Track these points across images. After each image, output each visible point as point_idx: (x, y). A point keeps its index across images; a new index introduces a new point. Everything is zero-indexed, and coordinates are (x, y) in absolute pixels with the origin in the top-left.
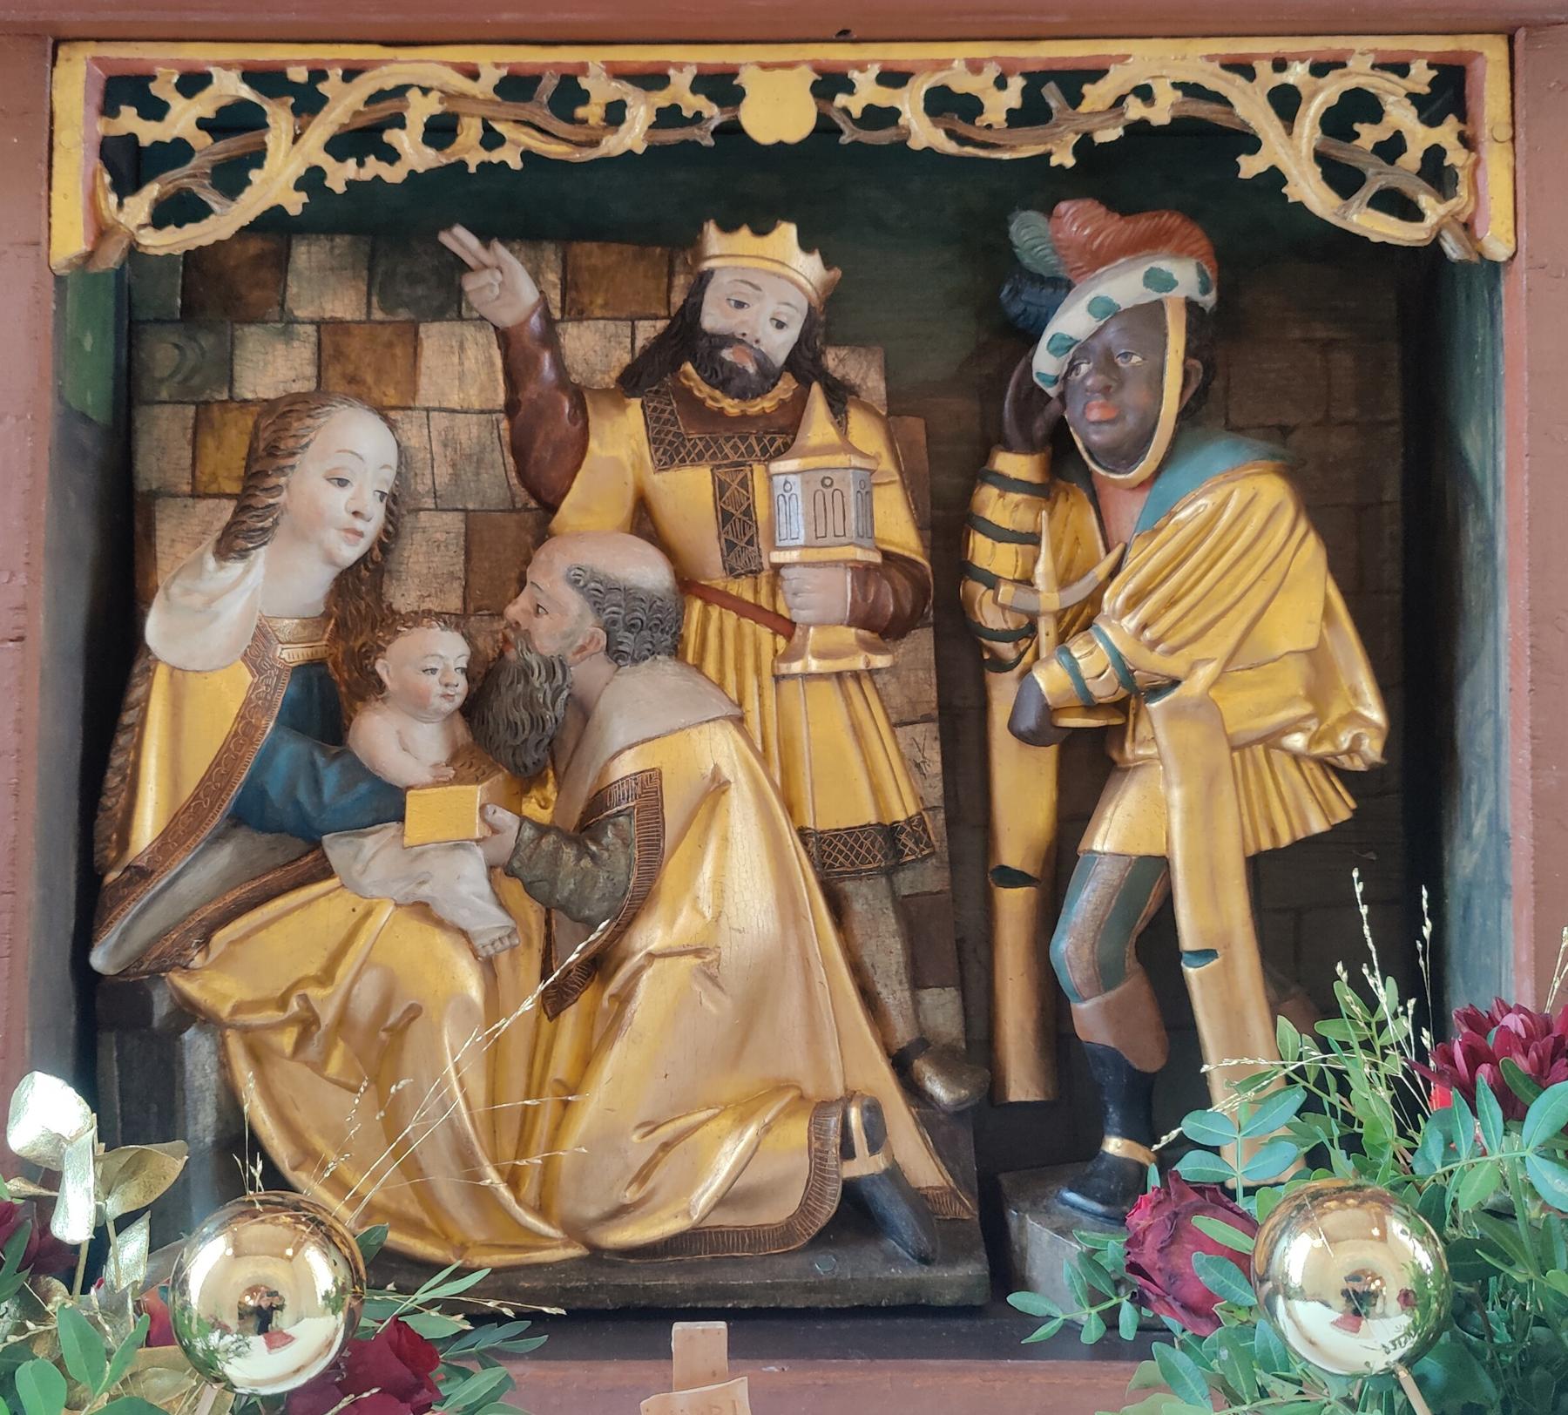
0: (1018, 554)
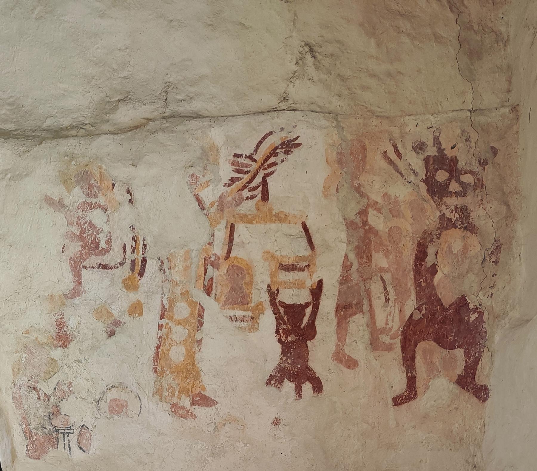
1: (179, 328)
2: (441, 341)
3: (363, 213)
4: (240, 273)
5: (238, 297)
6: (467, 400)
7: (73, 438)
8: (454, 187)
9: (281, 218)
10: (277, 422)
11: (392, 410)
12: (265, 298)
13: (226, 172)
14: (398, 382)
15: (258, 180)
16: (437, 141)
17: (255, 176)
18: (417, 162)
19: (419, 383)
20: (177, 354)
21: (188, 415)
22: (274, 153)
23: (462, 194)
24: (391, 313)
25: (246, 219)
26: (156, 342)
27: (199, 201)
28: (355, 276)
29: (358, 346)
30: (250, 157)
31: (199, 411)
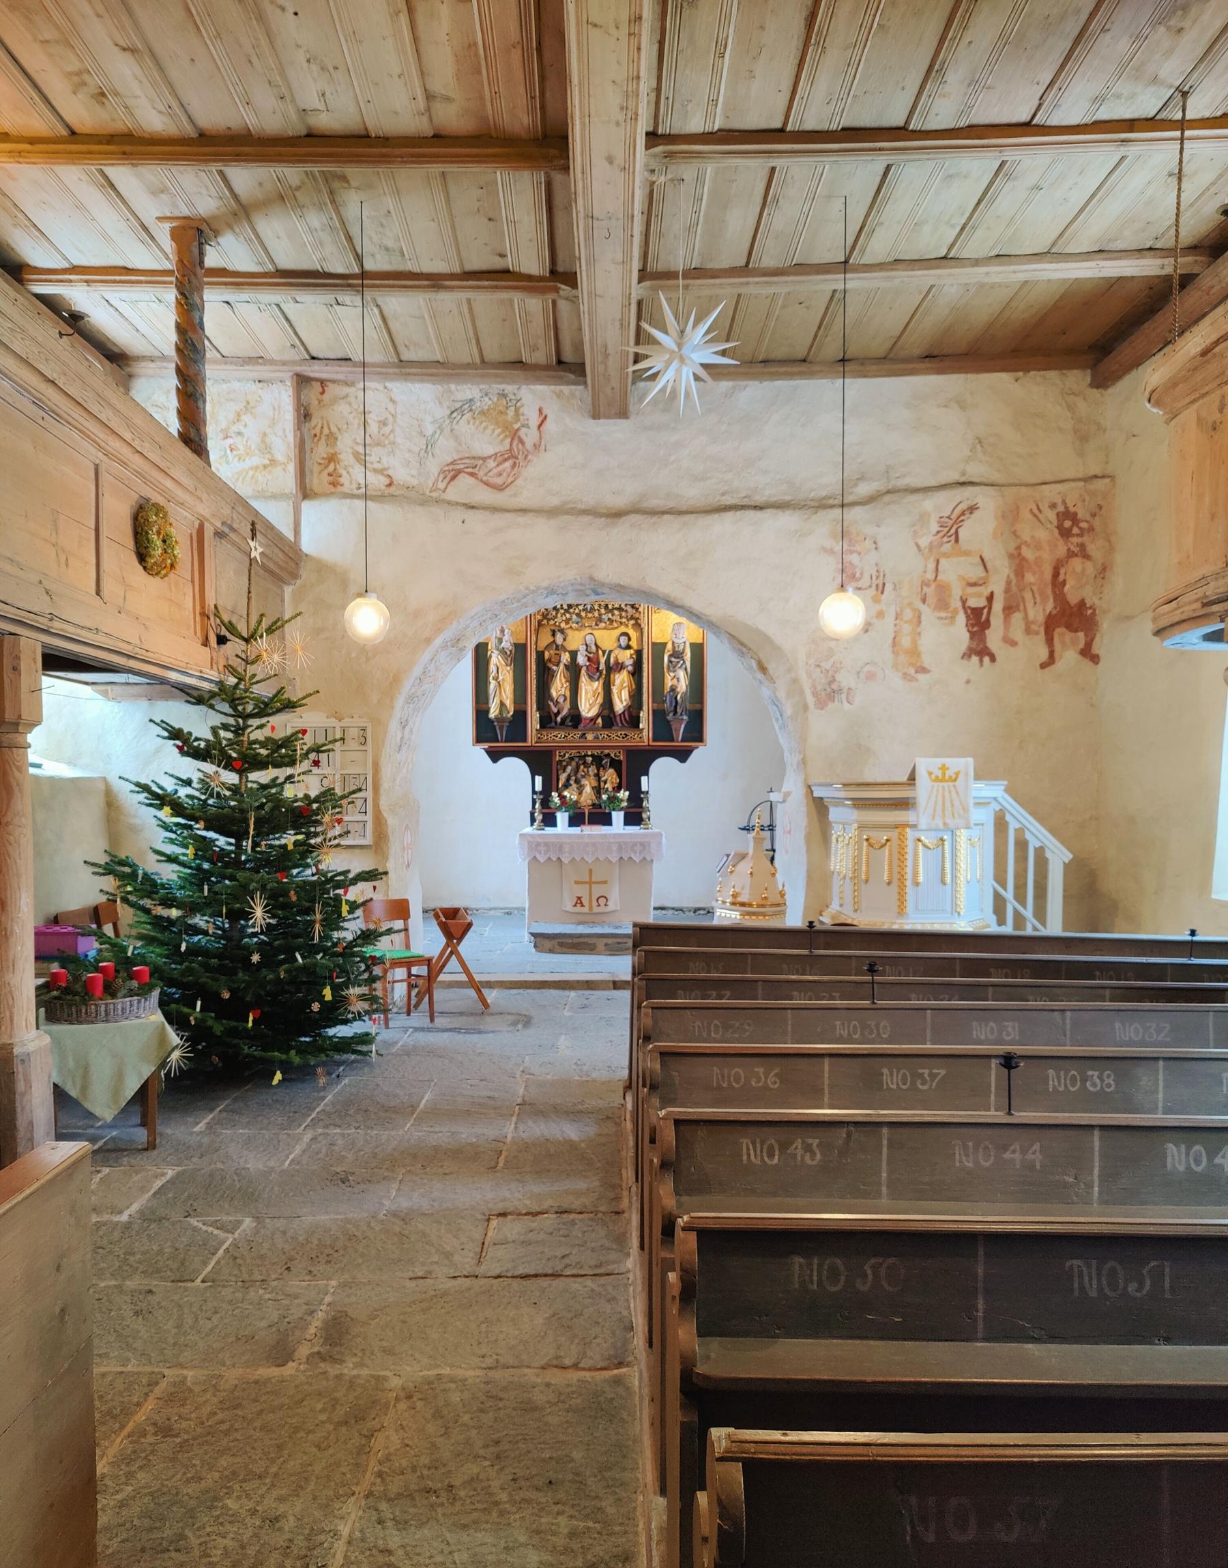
0: (601, 773)
1: (906, 626)
2: (1069, 627)
3: (1018, 548)
4: (943, 590)
5: (942, 604)
6: (1086, 664)
7: (844, 696)
8: (1075, 530)
9: (967, 553)
10: (968, 682)
11: (1040, 671)
12: (959, 604)
13: (934, 527)
14: (1044, 654)
15: (953, 531)
16: (1064, 503)
17: (951, 530)
18: (1051, 515)
19: (1056, 655)
20: (906, 642)
21: (912, 679)
22: (963, 514)
23: (1081, 535)
24: (1038, 612)
25: (946, 555)
26: (893, 635)
27: (918, 546)
28: (1014, 588)
29: (1017, 632)
30: (949, 517)
31: (921, 677)
